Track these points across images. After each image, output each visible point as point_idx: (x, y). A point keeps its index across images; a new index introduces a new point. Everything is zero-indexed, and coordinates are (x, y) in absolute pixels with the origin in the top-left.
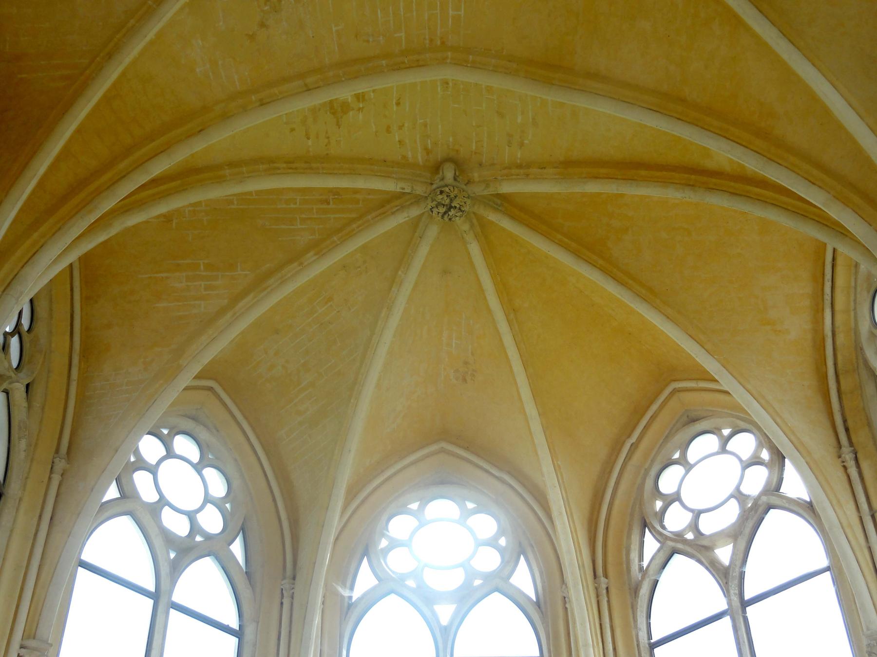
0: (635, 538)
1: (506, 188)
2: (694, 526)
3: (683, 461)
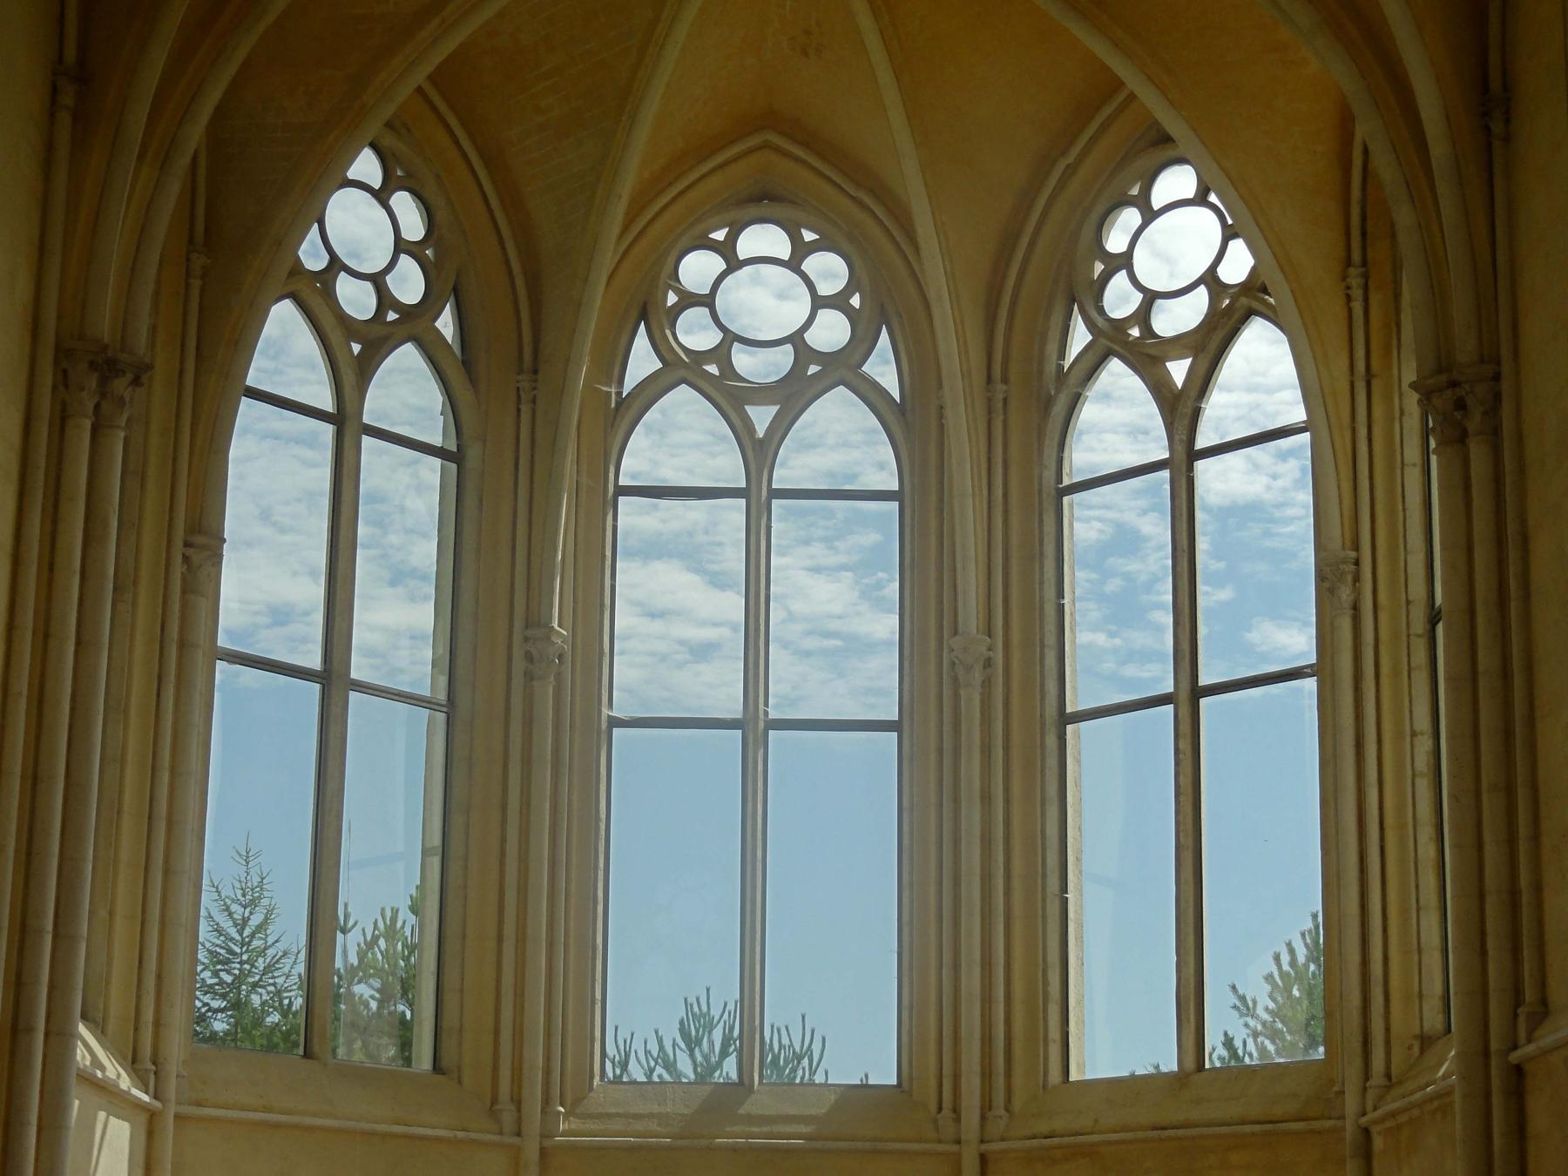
2: (1143, 316)
3: (1143, 203)
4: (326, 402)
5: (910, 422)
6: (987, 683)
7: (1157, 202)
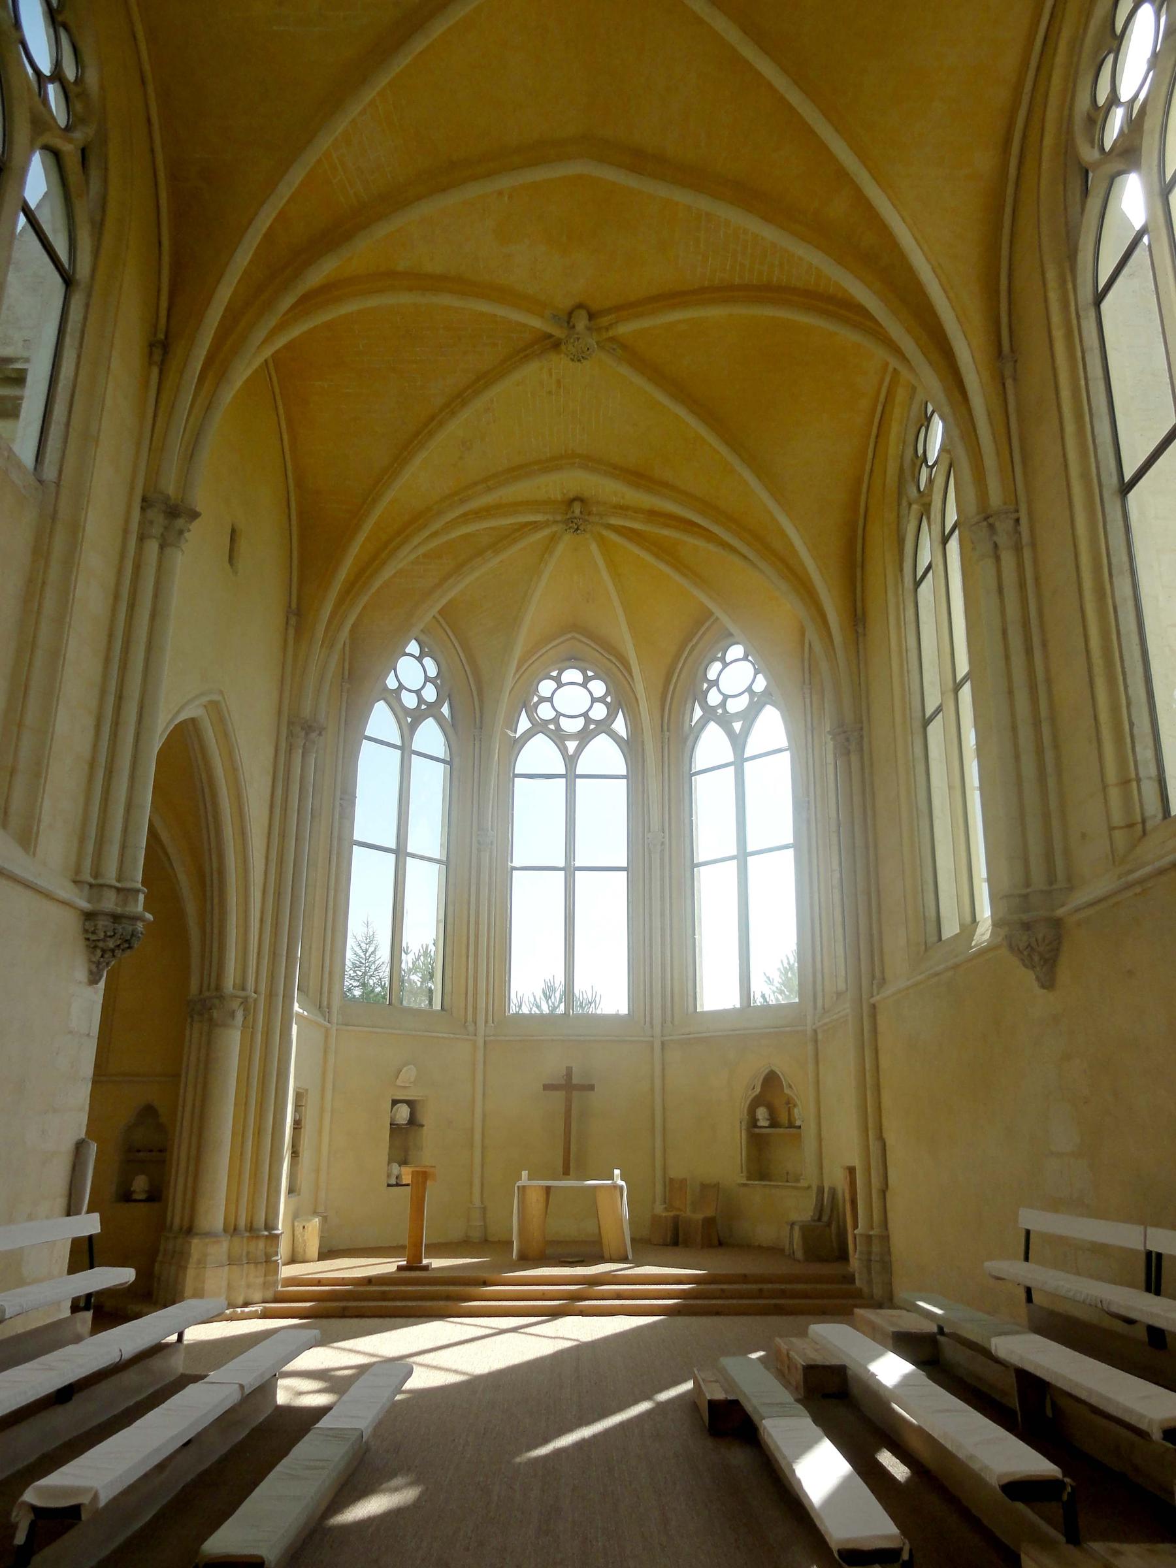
0: (689, 706)
1: (613, 521)
2: (723, 704)
3: (723, 660)
4: (399, 743)
5: (631, 747)
6: (662, 851)
7: (728, 659)
